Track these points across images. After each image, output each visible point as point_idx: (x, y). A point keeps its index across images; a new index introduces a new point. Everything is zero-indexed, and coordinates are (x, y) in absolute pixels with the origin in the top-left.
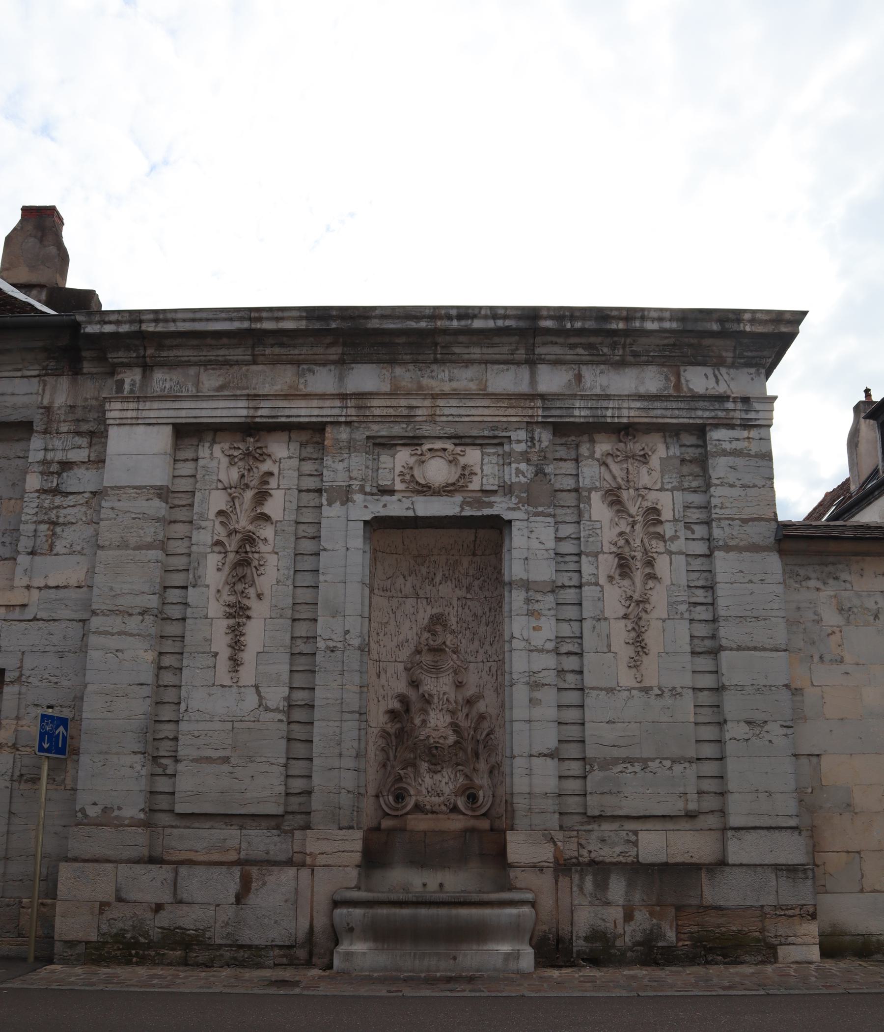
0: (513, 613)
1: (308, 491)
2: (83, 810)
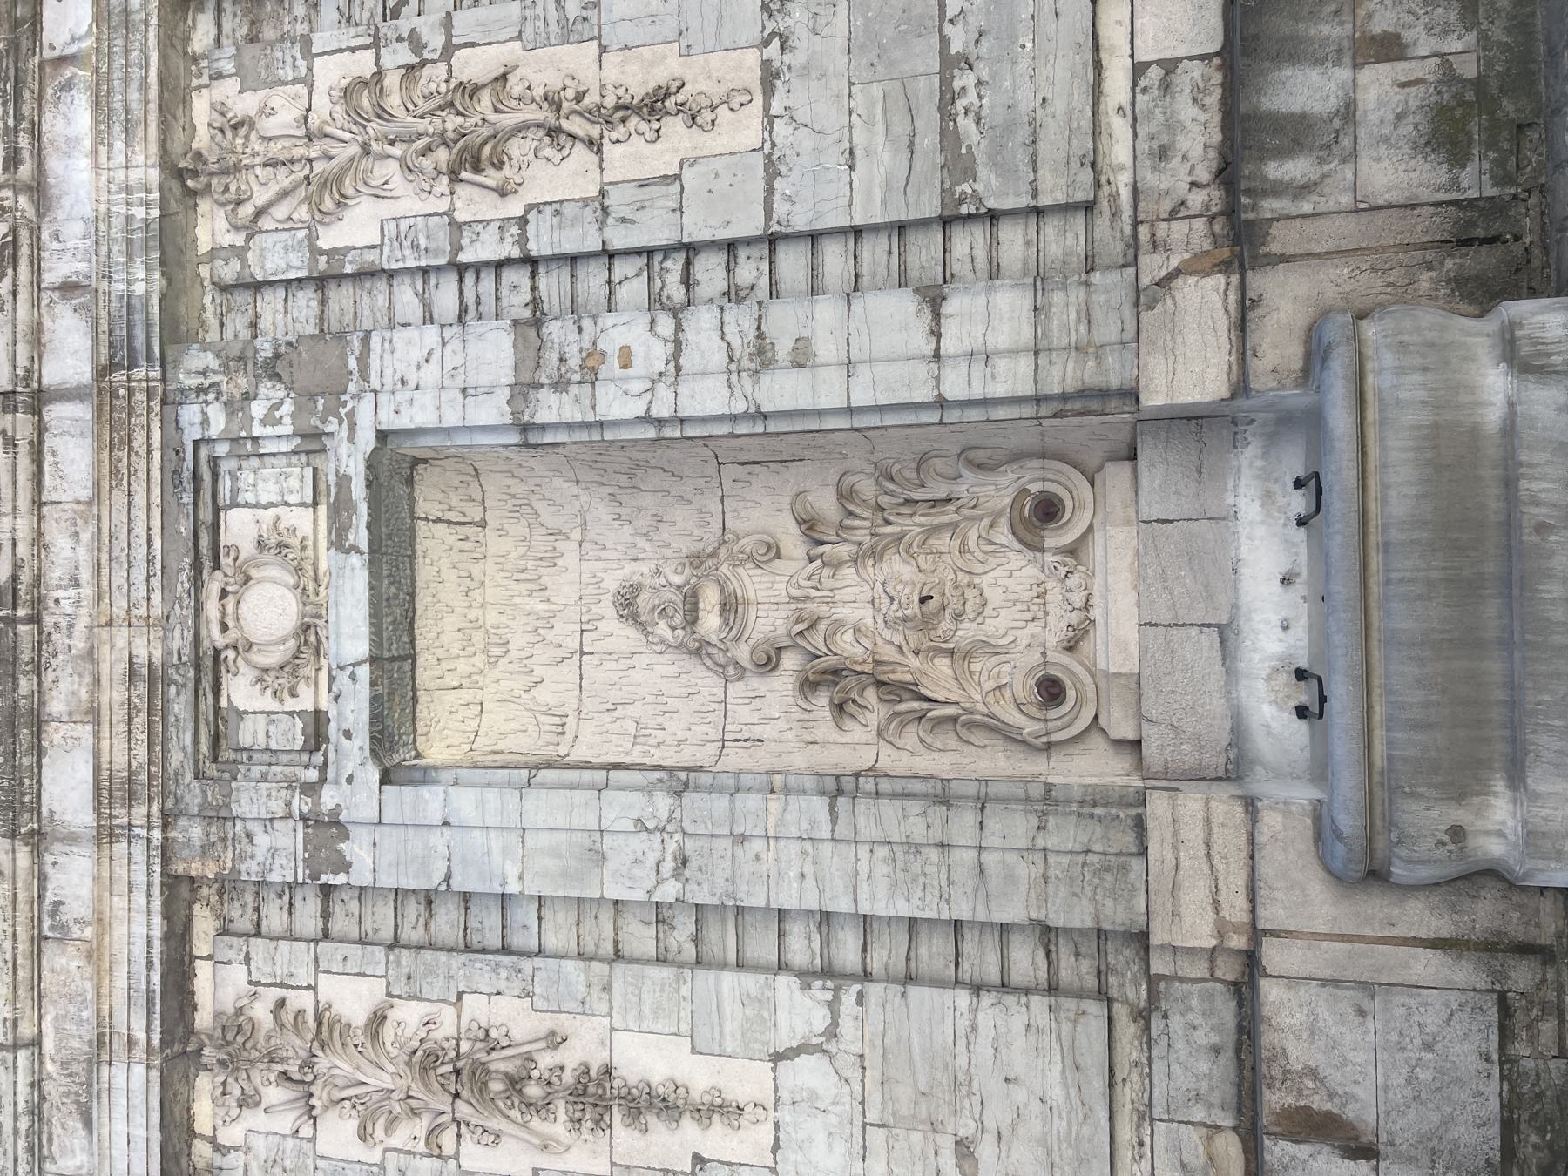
0: (590, 418)
1: (326, 915)
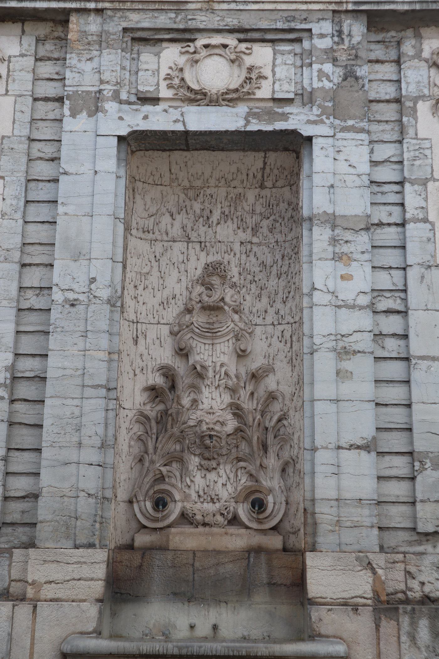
0: (315, 257)
1: (46, 99)
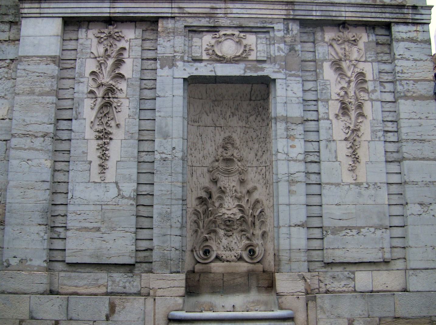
0: (278, 137)
1: (148, 59)
2: (7, 261)
